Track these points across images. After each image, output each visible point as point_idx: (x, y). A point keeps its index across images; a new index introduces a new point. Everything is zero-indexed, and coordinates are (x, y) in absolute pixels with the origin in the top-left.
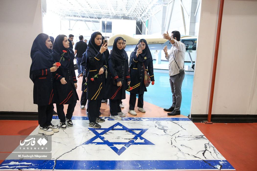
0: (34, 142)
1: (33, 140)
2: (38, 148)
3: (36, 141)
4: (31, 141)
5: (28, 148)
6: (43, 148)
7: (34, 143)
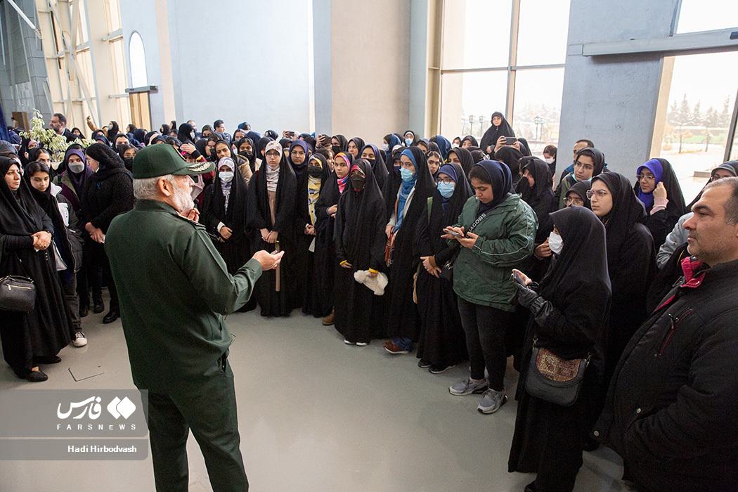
0: (98, 408)
1: (95, 402)
2: (110, 427)
3: (104, 405)
4: (88, 405)
5: (80, 427)
6: (122, 427)
7: (97, 413)
